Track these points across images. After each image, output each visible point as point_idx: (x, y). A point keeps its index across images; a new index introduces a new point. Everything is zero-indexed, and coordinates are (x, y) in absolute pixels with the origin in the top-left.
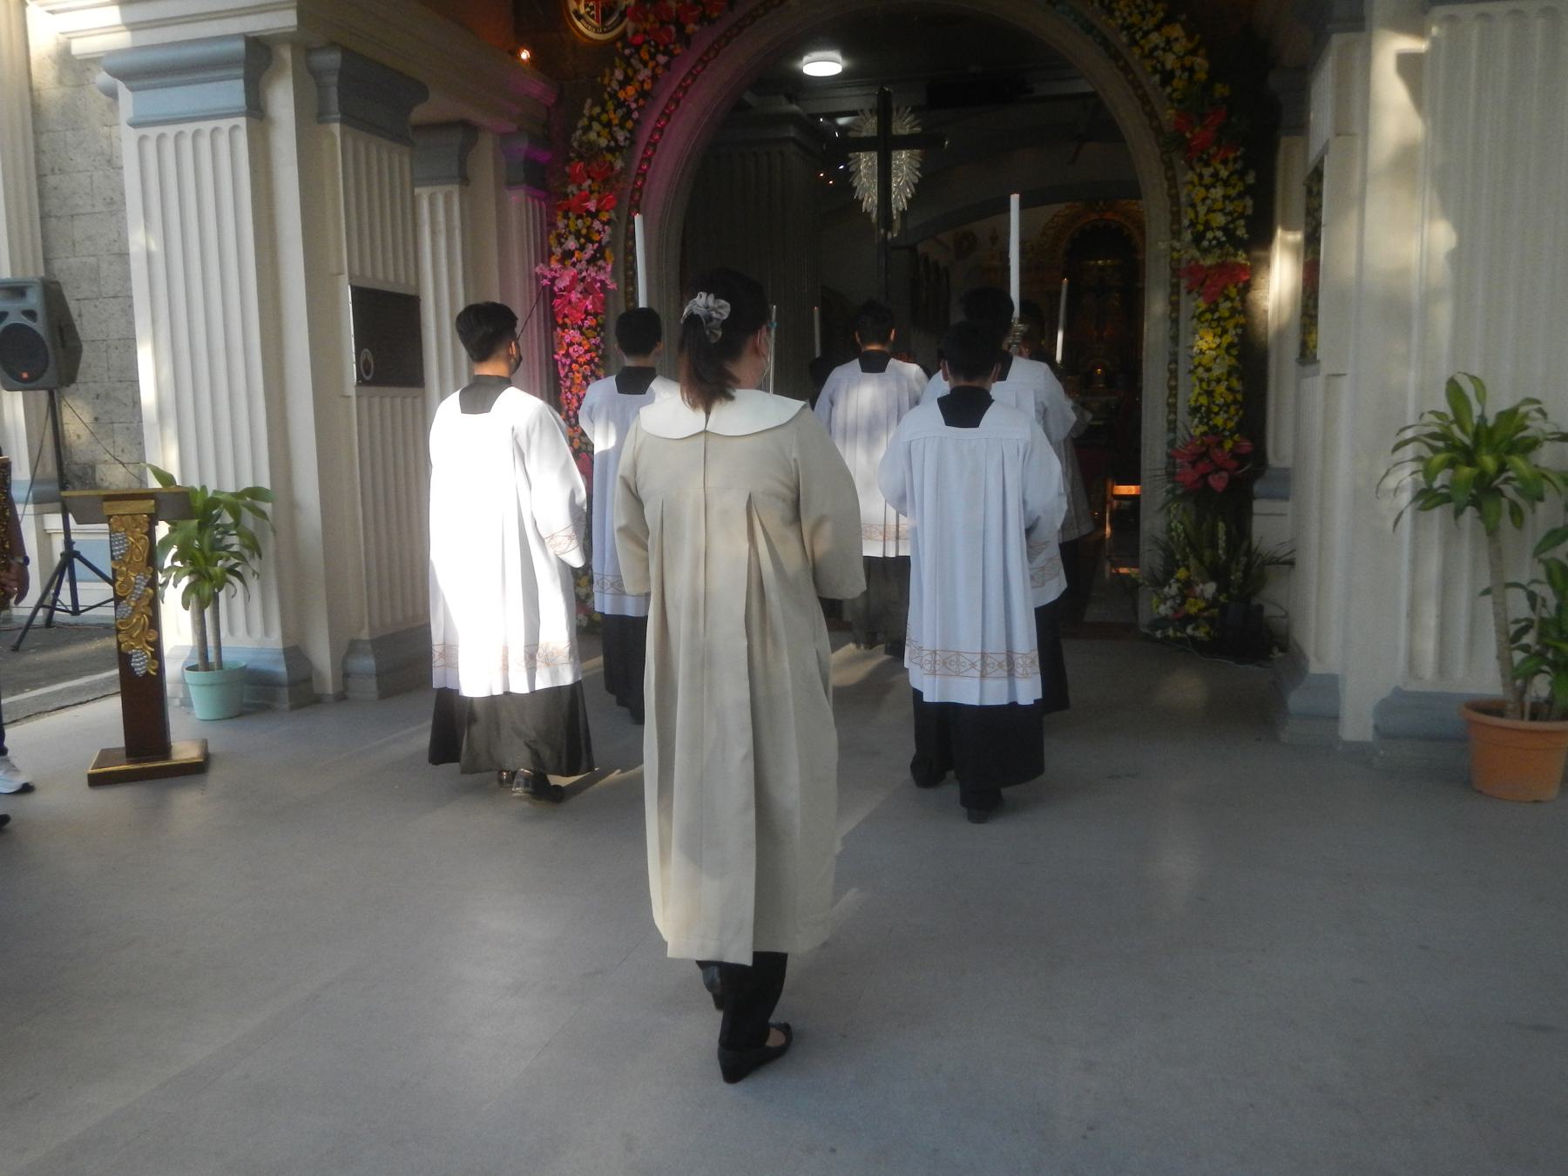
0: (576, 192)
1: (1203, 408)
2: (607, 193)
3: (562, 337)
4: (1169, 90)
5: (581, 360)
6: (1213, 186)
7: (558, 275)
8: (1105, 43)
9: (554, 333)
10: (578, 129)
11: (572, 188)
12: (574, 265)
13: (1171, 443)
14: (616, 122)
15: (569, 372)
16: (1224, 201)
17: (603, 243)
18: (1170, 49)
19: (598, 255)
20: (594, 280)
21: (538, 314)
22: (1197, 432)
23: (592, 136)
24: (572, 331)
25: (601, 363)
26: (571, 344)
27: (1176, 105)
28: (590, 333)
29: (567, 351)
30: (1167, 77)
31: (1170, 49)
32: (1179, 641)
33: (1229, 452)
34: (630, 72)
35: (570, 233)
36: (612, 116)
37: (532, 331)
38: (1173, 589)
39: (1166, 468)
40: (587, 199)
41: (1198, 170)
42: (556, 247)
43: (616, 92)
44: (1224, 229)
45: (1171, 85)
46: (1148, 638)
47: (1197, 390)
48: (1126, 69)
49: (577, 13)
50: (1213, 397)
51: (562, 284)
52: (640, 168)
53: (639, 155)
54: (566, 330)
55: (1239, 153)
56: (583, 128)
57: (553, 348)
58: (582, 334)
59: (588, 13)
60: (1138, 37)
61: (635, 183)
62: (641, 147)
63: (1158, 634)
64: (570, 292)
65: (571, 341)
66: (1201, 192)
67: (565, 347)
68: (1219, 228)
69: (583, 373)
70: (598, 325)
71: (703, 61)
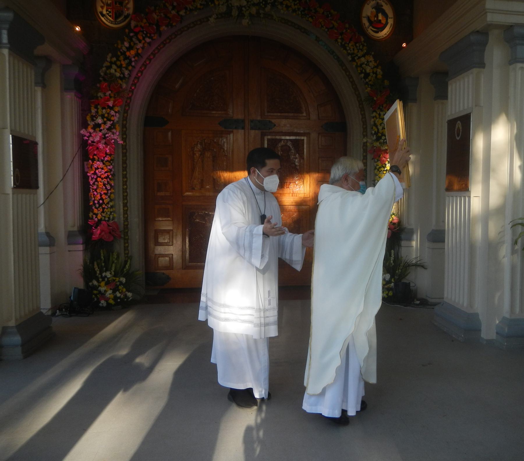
0: (102, 96)
3: (92, 165)
4: (367, 80)
9: (85, 163)
10: (103, 67)
11: (100, 94)
12: (101, 131)
14: (124, 66)
17: (115, 121)
18: (369, 65)
19: (112, 127)
23: (112, 71)
24: (98, 162)
26: (97, 168)
27: (370, 86)
28: (108, 164)
29: (95, 172)
31: (369, 65)
34: (132, 44)
36: (123, 62)
40: (109, 101)
49: (101, 13)
52: (131, 88)
56: (106, 67)
58: (104, 164)
60: (356, 58)
62: (132, 78)
64: (97, 143)
65: (98, 167)
67: (94, 170)
69: (103, 182)
70: (111, 160)
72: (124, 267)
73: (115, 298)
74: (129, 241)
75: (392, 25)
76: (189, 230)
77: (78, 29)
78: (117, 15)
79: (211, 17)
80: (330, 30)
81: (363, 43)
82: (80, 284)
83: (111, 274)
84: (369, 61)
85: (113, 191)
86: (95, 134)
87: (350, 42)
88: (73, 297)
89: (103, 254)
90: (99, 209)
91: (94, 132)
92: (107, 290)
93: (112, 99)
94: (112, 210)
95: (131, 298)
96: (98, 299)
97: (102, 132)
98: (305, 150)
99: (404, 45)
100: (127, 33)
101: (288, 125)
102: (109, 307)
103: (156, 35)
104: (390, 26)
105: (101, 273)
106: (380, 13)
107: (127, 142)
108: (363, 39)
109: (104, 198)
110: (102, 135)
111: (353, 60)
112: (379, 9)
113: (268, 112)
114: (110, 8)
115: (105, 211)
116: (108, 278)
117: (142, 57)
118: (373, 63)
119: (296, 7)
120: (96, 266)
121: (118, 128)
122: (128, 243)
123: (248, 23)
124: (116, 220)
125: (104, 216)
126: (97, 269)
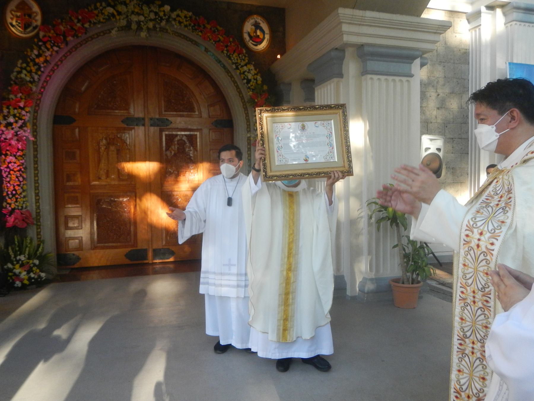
3: (5, 160)
4: (249, 85)
10: (14, 72)
11: (12, 96)
12: (13, 129)
14: (34, 71)
17: (26, 120)
18: (250, 73)
23: (23, 76)
24: (11, 157)
25: (24, 171)
26: (10, 163)
27: (251, 90)
28: (20, 158)
31: (250, 73)
34: (41, 52)
40: (20, 102)
43: (34, 59)
48: (232, 77)
52: (40, 90)
53: (40, 85)
58: (16, 158)
60: (239, 67)
62: (41, 82)
67: (7, 164)
69: (16, 175)
70: (24, 155)
71: (70, 52)
72: (37, 250)
73: (30, 279)
74: (41, 227)
75: (269, 40)
76: (97, 215)
78: (26, 26)
79: (112, 29)
80: (217, 43)
81: (245, 54)
83: (25, 257)
86: (7, 131)
87: (234, 54)
89: (18, 239)
90: (12, 199)
91: (7, 130)
92: (21, 271)
93: (24, 100)
94: (24, 200)
95: (44, 278)
96: (13, 280)
98: (198, 144)
99: (279, 56)
100: (36, 42)
101: (183, 123)
102: (24, 287)
103: (63, 44)
105: (15, 257)
108: (244, 51)
110: (14, 133)
111: (237, 68)
112: (257, 26)
113: (165, 111)
114: (18, 20)
115: (19, 201)
116: (22, 261)
117: (50, 63)
119: (188, 23)
121: (29, 126)
122: (40, 228)
123: (146, 35)
124: (29, 208)
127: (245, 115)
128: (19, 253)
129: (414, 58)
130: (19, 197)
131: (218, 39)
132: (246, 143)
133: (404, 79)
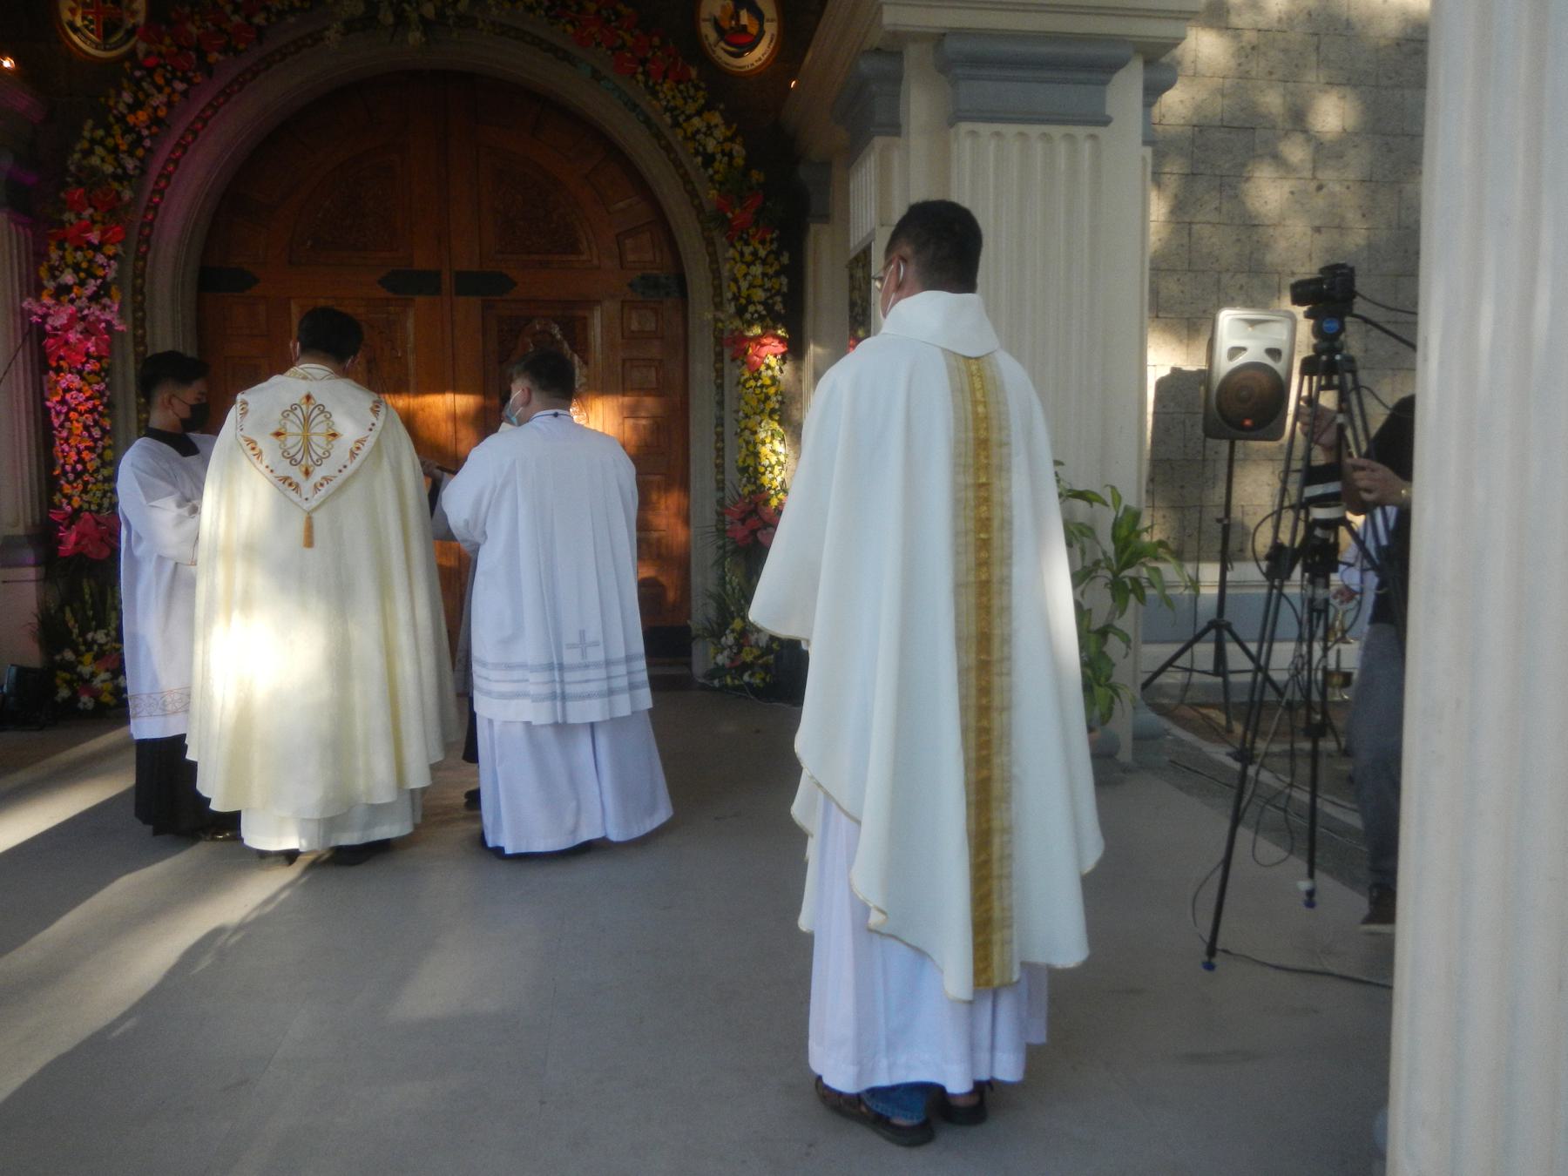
1: (751, 469)
2: (113, 226)
3: (57, 382)
4: (711, 171)
5: (80, 408)
6: (753, 263)
7: (51, 312)
8: (647, 121)
9: (45, 378)
11: (69, 216)
12: (72, 301)
13: (721, 502)
14: (124, 147)
15: (64, 421)
16: (763, 279)
18: (711, 135)
19: (102, 292)
20: (100, 321)
21: (24, 356)
22: (746, 491)
23: (95, 161)
24: (70, 375)
25: (106, 411)
26: (68, 390)
27: (717, 186)
28: (92, 378)
29: (63, 397)
30: (709, 160)
31: (711, 135)
32: (736, 688)
33: (775, 509)
34: (141, 96)
35: (68, 266)
36: (120, 142)
37: (17, 375)
38: (729, 639)
39: (716, 526)
40: (91, 231)
41: (739, 248)
42: (48, 281)
43: (124, 116)
44: (764, 303)
45: (713, 167)
46: (703, 687)
47: (744, 451)
49: (72, 25)
50: (759, 457)
51: (60, 320)
52: (150, 200)
53: (150, 186)
54: (62, 374)
55: (774, 235)
57: (42, 394)
58: (82, 378)
59: (86, 27)
60: (681, 119)
61: (145, 217)
63: (716, 683)
64: (66, 331)
66: (740, 269)
67: (61, 392)
68: (760, 303)
70: (102, 369)
77: (7, 63)
78: (108, 30)
79: (327, 28)
82: (32, 656)
83: (107, 635)
84: (712, 124)
85: (111, 442)
88: (8, 687)
91: (57, 304)
94: (106, 487)
97: (76, 303)
104: (768, 42)
105: (83, 633)
106: (743, 9)
107: (148, 329)
108: (694, 73)
109: (87, 458)
115: (91, 490)
116: (101, 645)
118: (723, 130)
120: (68, 615)
125: (87, 502)
126: (71, 623)
127: (708, 258)
128: (94, 623)
129: (1112, 67)
130: (92, 480)
131: (619, 42)
132: (712, 339)
133: (1080, 131)
